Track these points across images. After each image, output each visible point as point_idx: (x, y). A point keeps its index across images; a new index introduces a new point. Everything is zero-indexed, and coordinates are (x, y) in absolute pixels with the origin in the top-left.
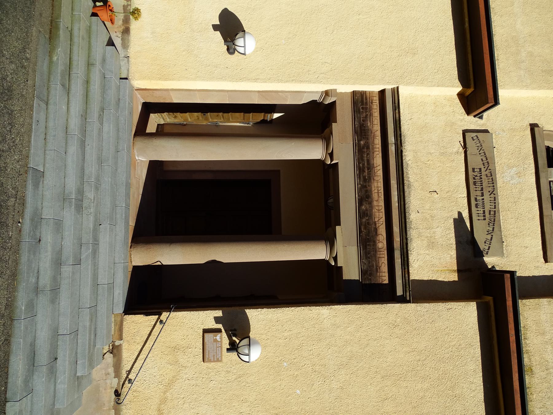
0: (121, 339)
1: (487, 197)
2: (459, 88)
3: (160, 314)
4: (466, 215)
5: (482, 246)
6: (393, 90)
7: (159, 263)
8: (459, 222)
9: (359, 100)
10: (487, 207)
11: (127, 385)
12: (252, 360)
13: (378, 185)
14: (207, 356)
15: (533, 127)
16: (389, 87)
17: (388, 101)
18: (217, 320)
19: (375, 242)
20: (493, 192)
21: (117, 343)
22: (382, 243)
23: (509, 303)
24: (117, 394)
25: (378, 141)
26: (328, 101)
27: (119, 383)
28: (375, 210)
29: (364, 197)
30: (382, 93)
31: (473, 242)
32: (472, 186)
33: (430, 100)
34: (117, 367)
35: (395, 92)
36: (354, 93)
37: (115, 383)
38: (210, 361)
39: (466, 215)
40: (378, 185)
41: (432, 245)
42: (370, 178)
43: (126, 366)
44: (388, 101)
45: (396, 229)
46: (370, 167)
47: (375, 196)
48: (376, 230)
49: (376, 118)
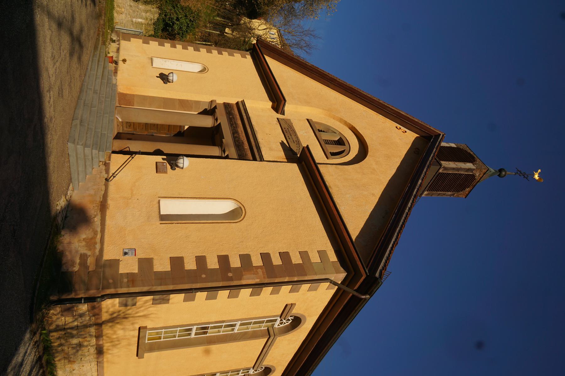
0: (110, 160)
1: (293, 136)
2: (271, 103)
3: (132, 155)
4: (285, 142)
5: (296, 151)
6: (242, 101)
7: (128, 149)
8: (282, 144)
9: (227, 106)
10: (295, 140)
11: (112, 177)
12: (184, 167)
13: (241, 129)
14: (159, 170)
15: (308, 120)
16: (240, 100)
17: (241, 107)
18: (163, 159)
19: (243, 147)
20: (296, 135)
21: (107, 162)
22: (246, 146)
23: (315, 168)
24: (106, 179)
25: (238, 117)
26: (213, 106)
27: (108, 176)
28: (241, 137)
29: (235, 132)
30: (237, 103)
31: (291, 149)
32: (285, 133)
33: (259, 106)
34: (107, 171)
35: (243, 102)
36: (224, 103)
37: (106, 176)
38: (160, 172)
39: (285, 142)
40: (241, 129)
41: (271, 149)
42: (236, 127)
43: (112, 171)
44: (241, 107)
45: (252, 140)
46: (236, 124)
47: (240, 132)
48: (243, 143)
49: (237, 113)
